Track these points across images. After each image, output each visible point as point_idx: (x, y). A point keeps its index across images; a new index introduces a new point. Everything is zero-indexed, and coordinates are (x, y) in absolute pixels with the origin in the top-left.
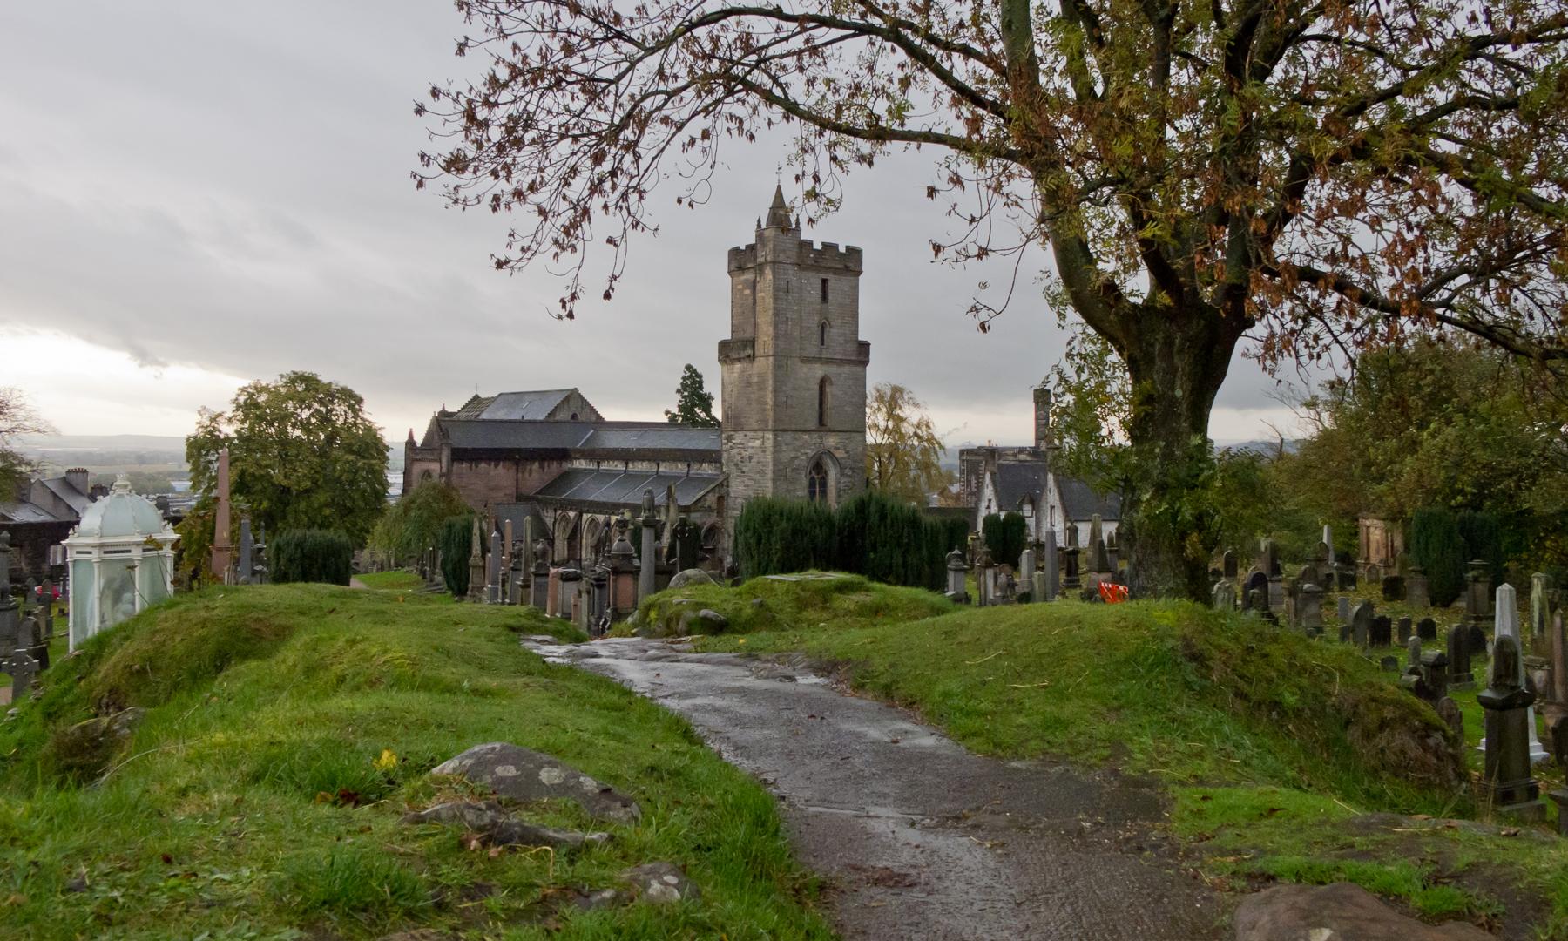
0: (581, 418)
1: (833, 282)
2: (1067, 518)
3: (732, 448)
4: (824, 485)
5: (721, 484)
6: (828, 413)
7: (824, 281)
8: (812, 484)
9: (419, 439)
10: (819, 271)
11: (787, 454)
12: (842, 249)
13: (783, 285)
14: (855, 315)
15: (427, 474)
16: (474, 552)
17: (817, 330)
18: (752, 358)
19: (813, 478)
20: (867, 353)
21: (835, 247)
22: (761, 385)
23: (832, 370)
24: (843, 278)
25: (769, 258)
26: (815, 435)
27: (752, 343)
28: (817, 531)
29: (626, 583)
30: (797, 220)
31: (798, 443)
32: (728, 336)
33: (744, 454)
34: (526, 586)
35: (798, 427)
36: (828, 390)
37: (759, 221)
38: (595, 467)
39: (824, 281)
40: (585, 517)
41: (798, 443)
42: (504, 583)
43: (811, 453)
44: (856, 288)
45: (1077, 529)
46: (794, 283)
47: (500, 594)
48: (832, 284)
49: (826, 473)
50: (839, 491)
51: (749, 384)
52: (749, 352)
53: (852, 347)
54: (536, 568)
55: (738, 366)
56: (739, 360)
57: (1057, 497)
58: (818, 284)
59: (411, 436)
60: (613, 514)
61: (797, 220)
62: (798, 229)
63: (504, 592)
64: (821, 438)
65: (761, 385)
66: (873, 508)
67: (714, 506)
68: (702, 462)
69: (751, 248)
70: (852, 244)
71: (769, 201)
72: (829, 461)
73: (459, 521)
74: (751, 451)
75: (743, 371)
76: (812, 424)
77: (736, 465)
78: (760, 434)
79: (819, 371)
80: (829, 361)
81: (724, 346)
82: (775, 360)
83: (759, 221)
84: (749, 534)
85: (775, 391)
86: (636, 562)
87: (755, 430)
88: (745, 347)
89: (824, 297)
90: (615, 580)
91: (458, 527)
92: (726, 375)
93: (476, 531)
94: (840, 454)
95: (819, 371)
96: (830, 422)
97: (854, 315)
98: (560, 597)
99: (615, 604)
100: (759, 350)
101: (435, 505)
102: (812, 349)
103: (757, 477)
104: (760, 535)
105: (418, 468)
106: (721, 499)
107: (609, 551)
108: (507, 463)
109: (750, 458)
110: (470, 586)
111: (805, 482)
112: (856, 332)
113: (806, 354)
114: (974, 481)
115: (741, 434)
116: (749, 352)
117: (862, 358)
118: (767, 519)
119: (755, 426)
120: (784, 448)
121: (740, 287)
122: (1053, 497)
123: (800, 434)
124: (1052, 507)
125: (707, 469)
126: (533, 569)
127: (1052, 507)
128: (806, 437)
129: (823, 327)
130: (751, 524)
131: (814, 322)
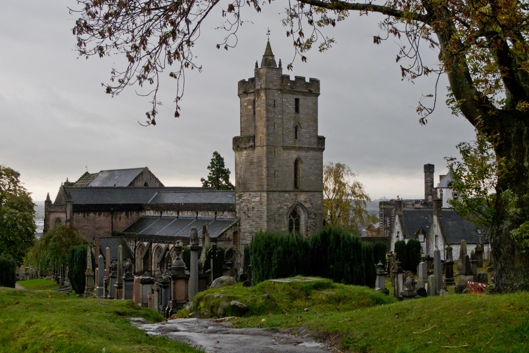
0: (150, 185)
1: (303, 101)
2: (445, 243)
3: (242, 202)
4: (298, 224)
5: (235, 225)
6: (301, 181)
7: (297, 100)
8: (291, 224)
9: (53, 199)
10: (293, 94)
11: (275, 206)
12: (307, 80)
13: (272, 102)
14: (316, 121)
15: (58, 220)
16: (88, 267)
17: (293, 130)
18: (253, 147)
19: (291, 220)
20: (323, 144)
21: (303, 79)
22: (260, 162)
23: (303, 154)
24: (308, 98)
25: (263, 86)
26: (292, 194)
27: (253, 138)
28: (298, 252)
29: (181, 284)
30: (280, 62)
31: (282, 199)
32: (238, 134)
34: (120, 287)
35: (282, 190)
36: (300, 166)
37: (257, 64)
38: (159, 215)
39: (297, 100)
40: (154, 245)
41: (282, 199)
42: (106, 285)
43: (290, 205)
44: (316, 104)
45: (451, 249)
46: (278, 100)
47: (104, 292)
48: (301, 102)
49: (299, 217)
50: (307, 227)
51: (252, 163)
52: (251, 143)
53: (314, 140)
54: (126, 276)
55: (245, 152)
56: (246, 149)
57: (439, 230)
58: (293, 102)
59: (48, 197)
60: (171, 243)
61: (280, 62)
62: (280, 68)
63: (107, 291)
64: (296, 195)
65: (260, 162)
66: (332, 237)
67: (232, 238)
68: (224, 211)
69: (252, 80)
70: (313, 77)
71: (263, 52)
72: (301, 209)
73: (78, 248)
74: (253, 204)
75: (248, 156)
76: (291, 187)
77: (245, 212)
78: (259, 193)
79: (294, 155)
80: (300, 149)
81: (236, 140)
82: (267, 148)
83: (257, 64)
84: (257, 255)
85: (268, 167)
86: (187, 272)
87: (256, 191)
88: (249, 141)
89: (297, 109)
90: (174, 283)
91: (77, 252)
92: (238, 158)
93: (89, 254)
94: (307, 205)
95: (294, 155)
96: (302, 187)
97: (315, 121)
98: (141, 294)
99: (174, 296)
100: (258, 143)
101: (64, 239)
102: (290, 141)
103: (258, 220)
104: (263, 255)
105: (53, 217)
106: (235, 233)
107: (170, 266)
108: (106, 214)
109: (253, 208)
110: (86, 287)
111: (286, 222)
112: (316, 131)
113: (286, 144)
114: (388, 221)
115: (248, 194)
117: (320, 147)
118: (267, 245)
120: (274, 202)
121: (245, 104)
122: (436, 230)
123: (283, 193)
124: (436, 236)
125: (227, 215)
126: (124, 277)
127: (436, 236)
128: (287, 195)
129: (296, 128)
130: (258, 248)
131: (291, 125)
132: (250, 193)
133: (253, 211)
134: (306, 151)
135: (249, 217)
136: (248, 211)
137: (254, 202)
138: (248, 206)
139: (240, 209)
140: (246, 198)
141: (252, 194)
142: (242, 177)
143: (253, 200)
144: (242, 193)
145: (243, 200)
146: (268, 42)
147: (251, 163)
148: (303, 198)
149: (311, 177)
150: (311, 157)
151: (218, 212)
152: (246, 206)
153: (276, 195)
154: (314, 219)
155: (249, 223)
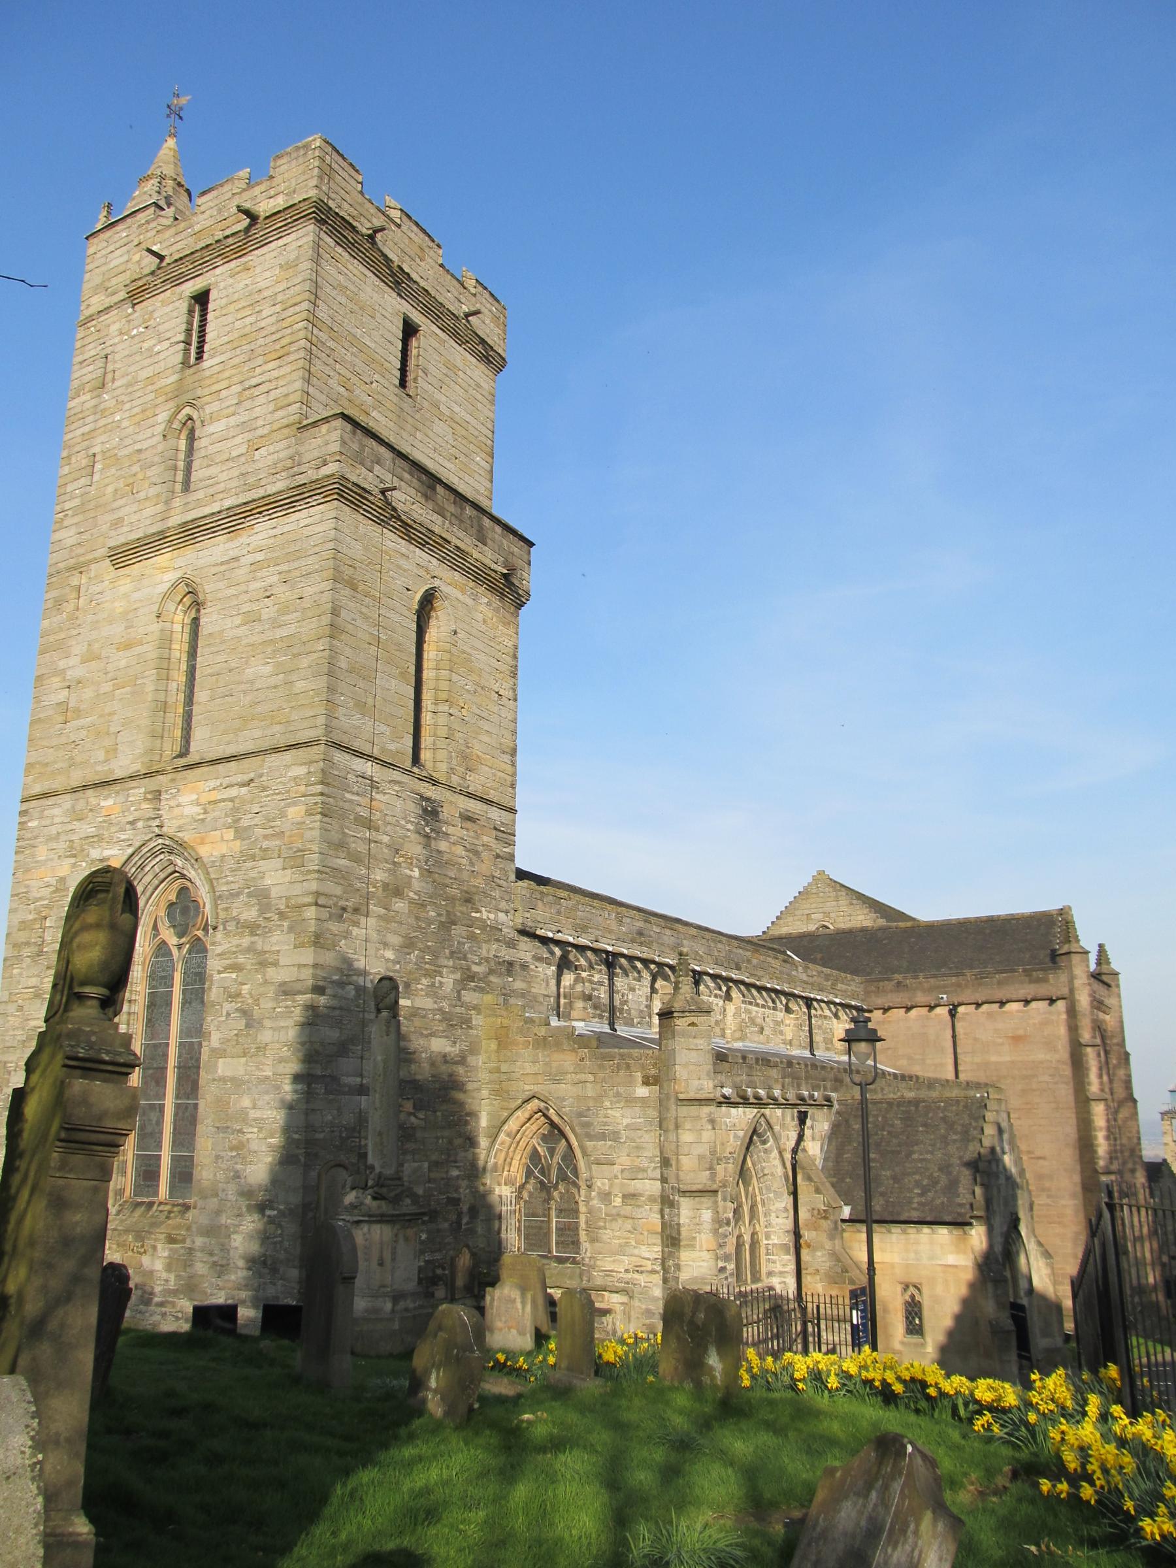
31: (85, 829)
41: (85, 829)
64: (157, 795)
80: (191, 532)
113: (119, 538)
134: (232, 531)
148: (197, 803)
149: (249, 672)
150: (259, 556)
153: (56, 811)
154: (252, 928)
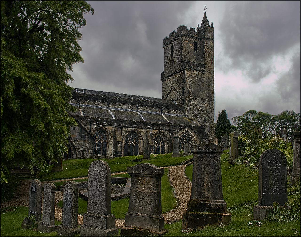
18: (203, 72)
33: (198, 108)
51: (201, 81)
55: (195, 72)
56: (197, 70)
74: (202, 107)
77: (194, 112)
87: (205, 100)
116: (202, 69)
119: (205, 98)
132: (199, 100)
133: (202, 112)
135: (199, 116)
136: (198, 111)
137: (203, 106)
138: (197, 108)
139: (190, 110)
140: (195, 103)
141: (201, 101)
142: (192, 89)
143: (202, 105)
144: (191, 99)
145: (192, 103)
146: (205, 14)
147: (200, 80)
151: (163, 109)
152: (195, 108)
155: (198, 120)
